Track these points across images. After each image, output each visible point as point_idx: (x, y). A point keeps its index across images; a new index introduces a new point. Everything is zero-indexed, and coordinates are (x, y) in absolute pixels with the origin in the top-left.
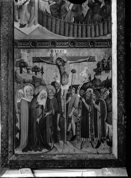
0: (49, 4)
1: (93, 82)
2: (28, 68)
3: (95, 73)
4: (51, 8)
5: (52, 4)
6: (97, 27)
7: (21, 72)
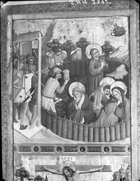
0: (55, 101)
2: (30, 178)
4: (57, 106)
5: (57, 101)
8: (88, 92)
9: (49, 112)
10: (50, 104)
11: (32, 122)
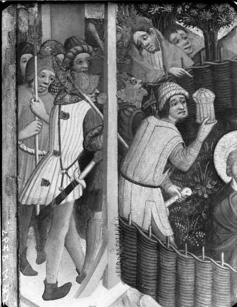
0: (167, 196)
4: (175, 214)
5: (176, 198)
9: (148, 234)
11: (87, 272)
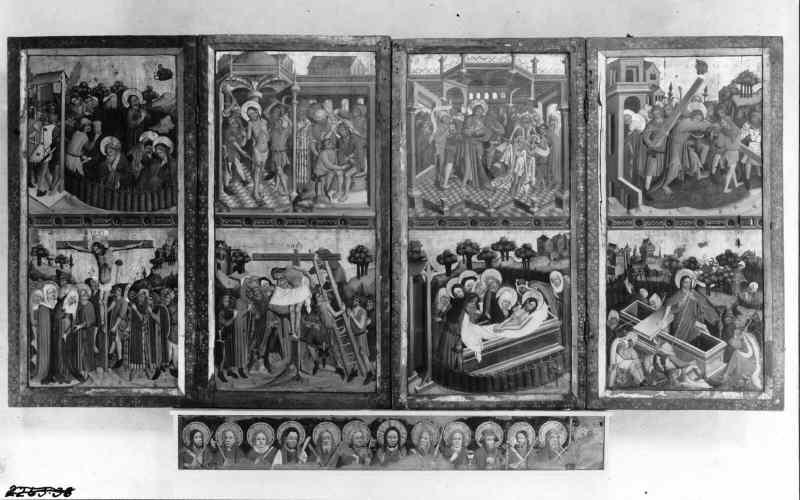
0: (82, 160)
1: (149, 280)
3: (151, 265)
6: (156, 197)
7: (39, 264)
8: (125, 149)
10: (76, 164)
